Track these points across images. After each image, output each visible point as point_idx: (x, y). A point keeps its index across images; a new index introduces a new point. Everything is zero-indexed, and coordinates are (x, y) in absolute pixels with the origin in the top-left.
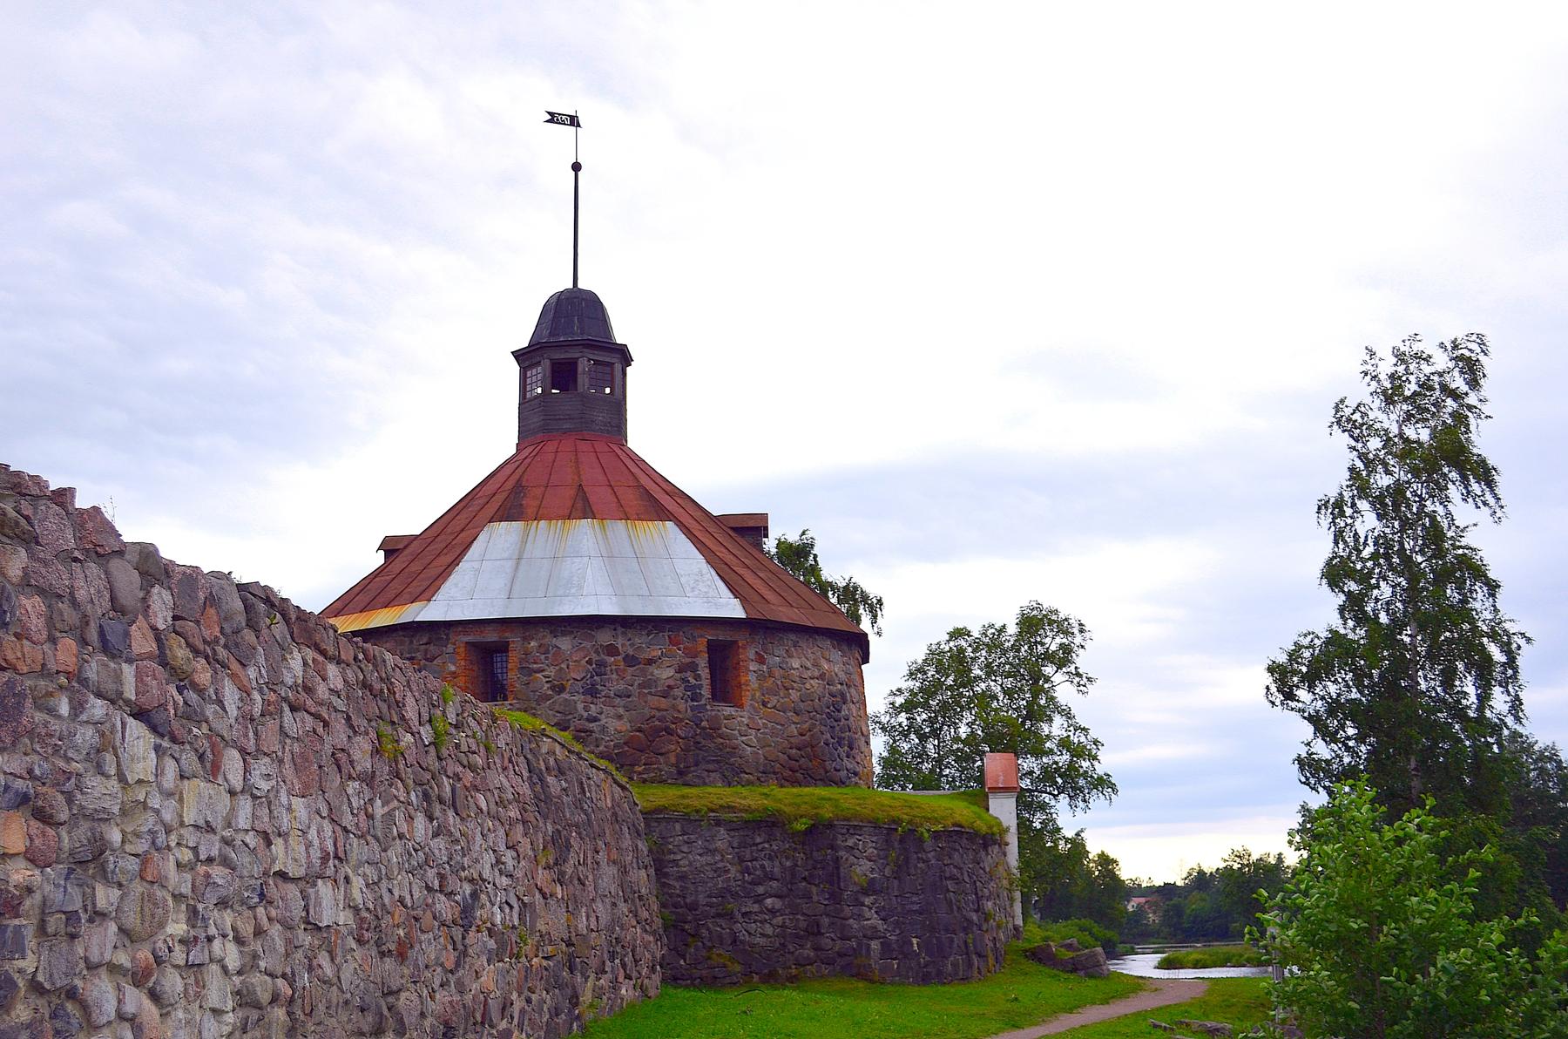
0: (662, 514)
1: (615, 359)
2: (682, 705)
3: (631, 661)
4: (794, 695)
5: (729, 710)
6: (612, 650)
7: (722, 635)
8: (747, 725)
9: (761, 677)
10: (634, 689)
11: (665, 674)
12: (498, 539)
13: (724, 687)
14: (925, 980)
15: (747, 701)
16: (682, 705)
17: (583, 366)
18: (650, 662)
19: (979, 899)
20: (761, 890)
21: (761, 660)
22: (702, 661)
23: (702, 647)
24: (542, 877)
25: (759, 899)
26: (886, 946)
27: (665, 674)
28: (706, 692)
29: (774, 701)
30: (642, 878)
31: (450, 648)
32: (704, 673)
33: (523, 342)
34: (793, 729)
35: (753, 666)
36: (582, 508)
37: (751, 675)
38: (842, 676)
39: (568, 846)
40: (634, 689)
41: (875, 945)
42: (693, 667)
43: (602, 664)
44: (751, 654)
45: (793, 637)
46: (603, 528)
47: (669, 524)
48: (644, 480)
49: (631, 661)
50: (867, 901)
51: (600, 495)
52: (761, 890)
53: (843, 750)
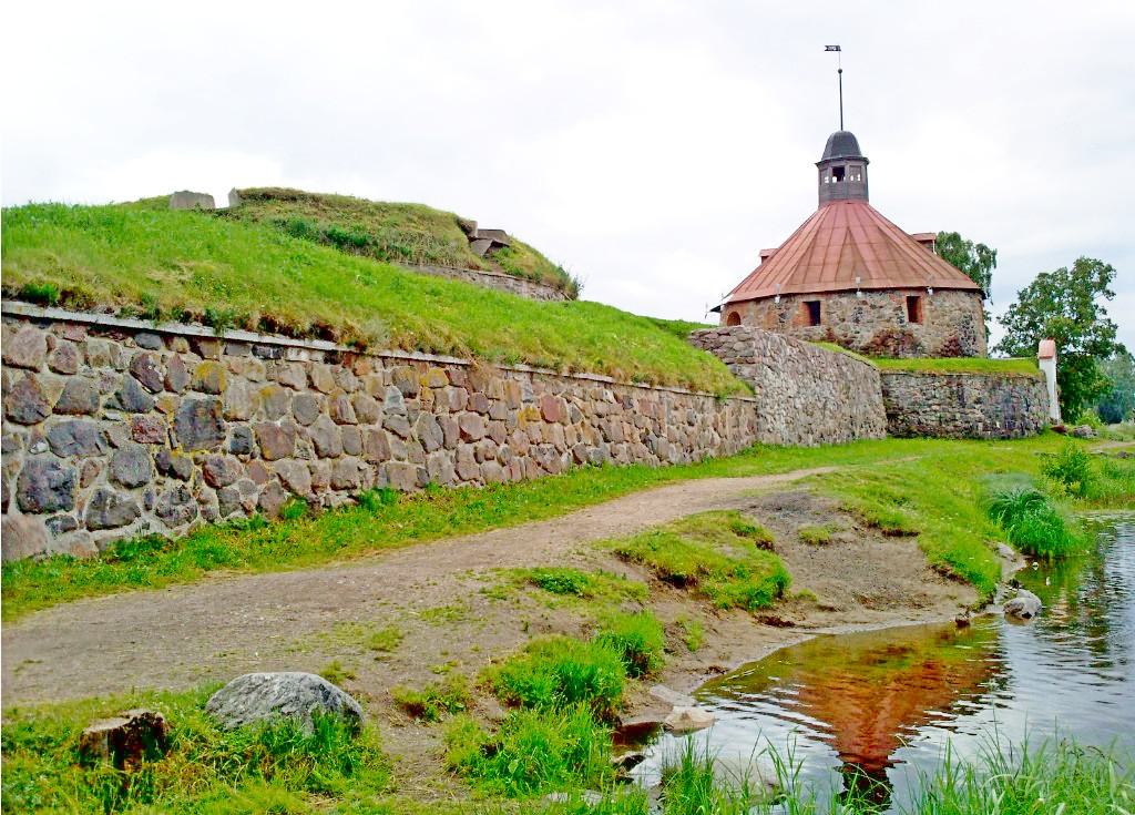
1: (862, 164)
2: (896, 325)
3: (873, 307)
4: (947, 318)
5: (914, 326)
6: (865, 303)
7: (913, 294)
8: (928, 333)
9: (932, 311)
11: (888, 312)
13: (913, 318)
14: (1003, 438)
15: (925, 322)
16: (896, 325)
17: (847, 169)
19: (1028, 406)
20: (930, 402)
21: (931, 304)
23: (904, 299)
24: (843, 397)
25: (930, 406)
26: (985, 429)
27: (888, 312)
28: (906, 319)
29: (937, 321)
30: (878, 399)
32: (905, 310)
34: (946, 334)
35: (928, 307)
37: (926, 308)
38: (970, 308)
39: (849, 388)
40: (875, 319)
41: (980, 425)
42: (900, 308)
43: (861, 309)
45: (945, 292)
48: (878, 222)
49: (873, 307)
50: (977, 406)
52: (930, 402)
53: (971, 341)
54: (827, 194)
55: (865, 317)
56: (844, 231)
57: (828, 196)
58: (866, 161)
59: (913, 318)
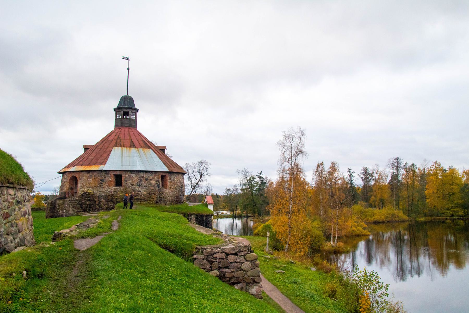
0: (149, 147)
5: (165, 190)
7: (164, 174)
10: (147, 185)
12: (116, 152)
17: (130, 113)
18: (150, 180)
22: (160, 180)
23: (160, 176)
27: (153, 182)
28: (161, 186)
31: (110, 175)
32: (160, 182)
33: (116, 107)
36: (132, 145)
40: (147, 185)
42: (158, 181)
44: (169, 178)
46: (138, 150)
47: (150, 149)
51: (135, 142)
54: (119, 124)
55: (144, 184)
56: (129, 141)
57: (119, 124)
58: (137, 110)
59: (163, 186)
